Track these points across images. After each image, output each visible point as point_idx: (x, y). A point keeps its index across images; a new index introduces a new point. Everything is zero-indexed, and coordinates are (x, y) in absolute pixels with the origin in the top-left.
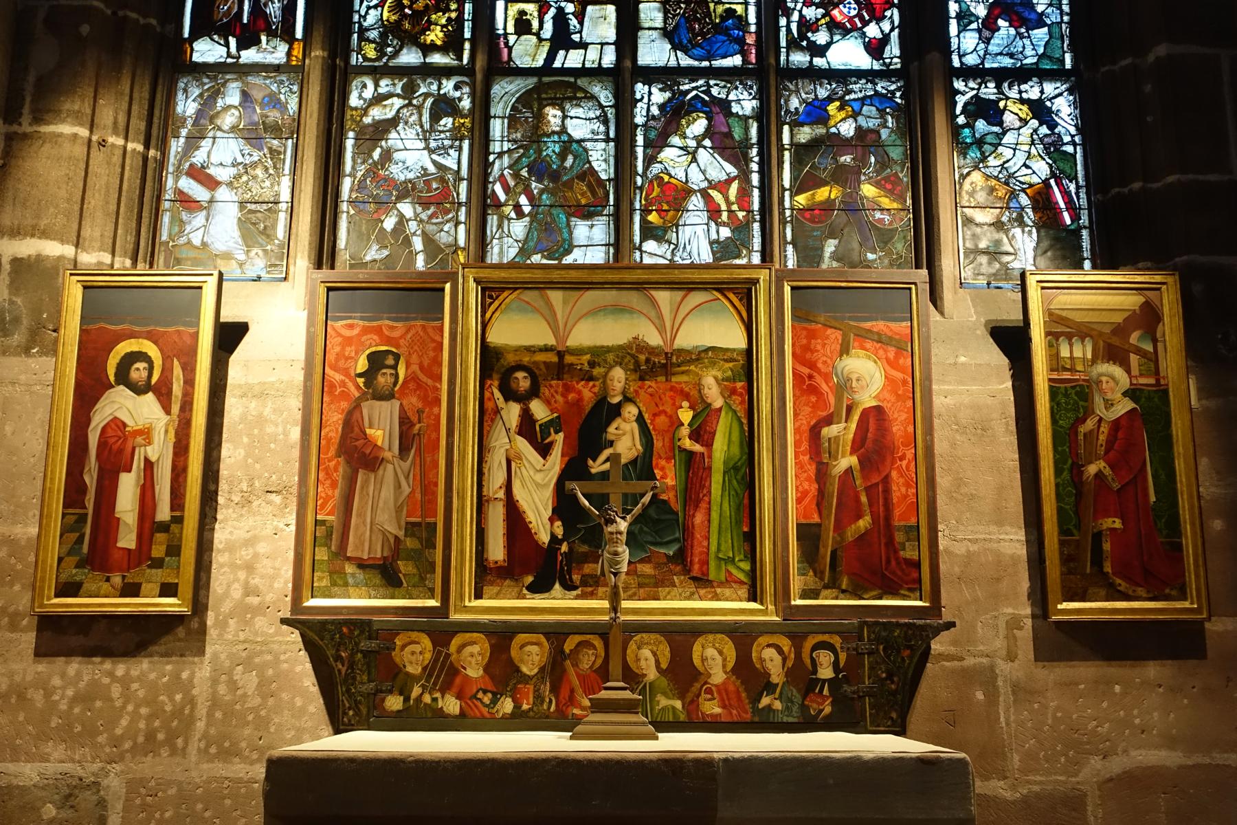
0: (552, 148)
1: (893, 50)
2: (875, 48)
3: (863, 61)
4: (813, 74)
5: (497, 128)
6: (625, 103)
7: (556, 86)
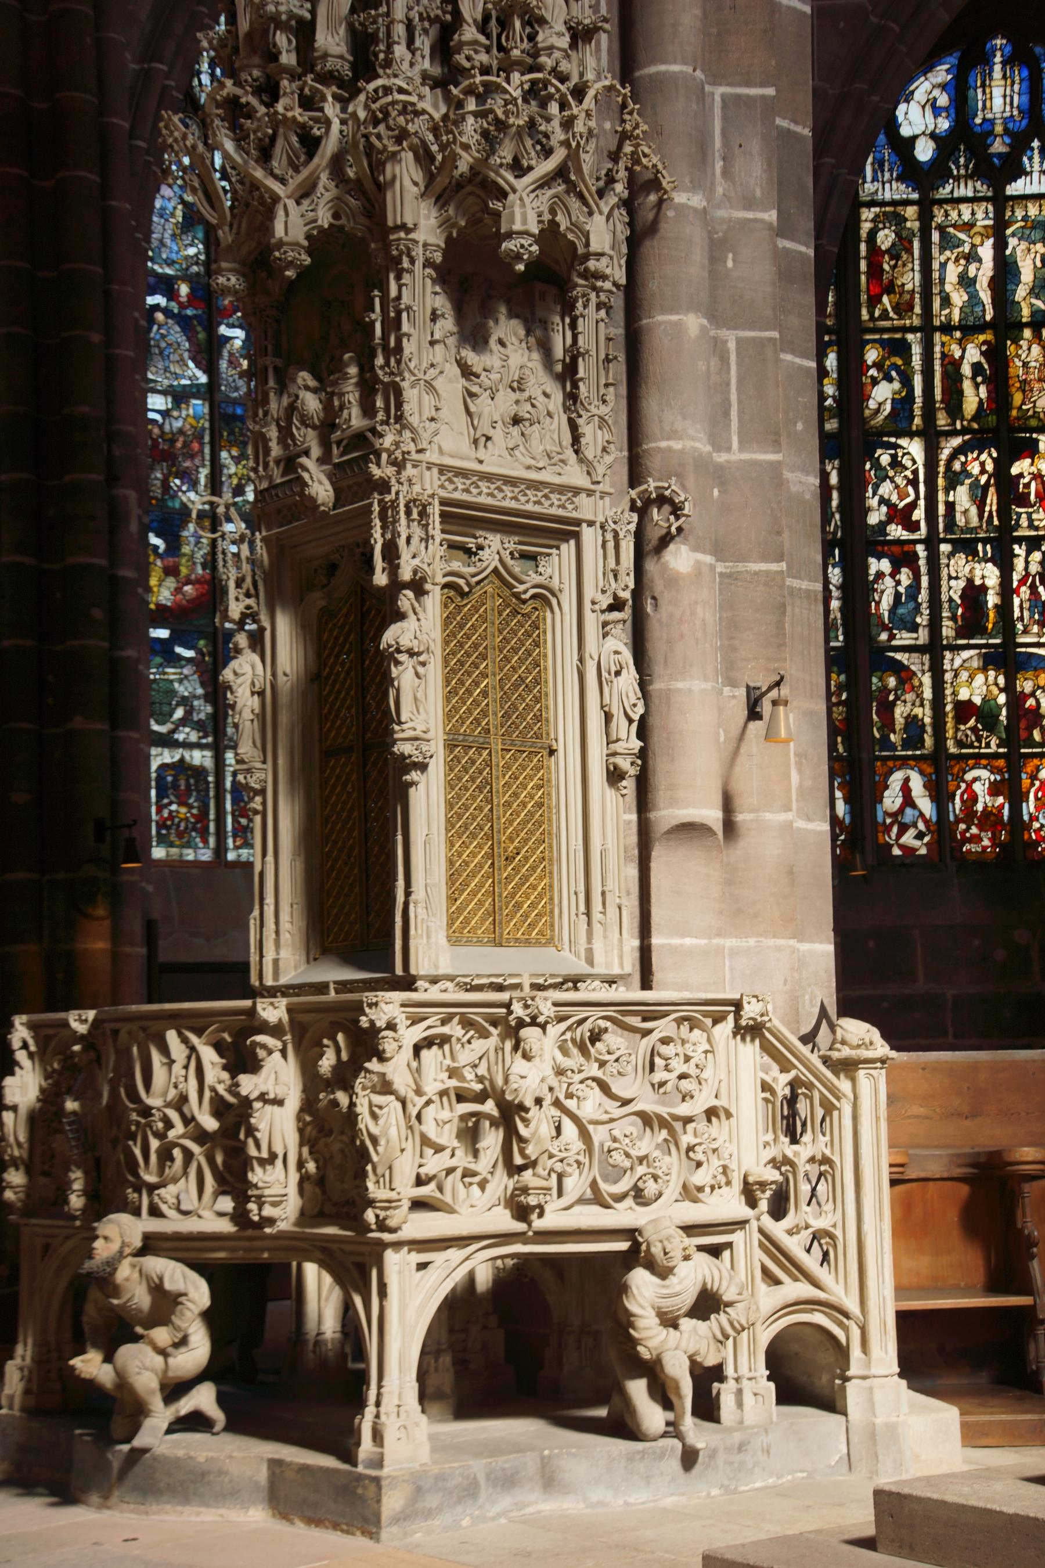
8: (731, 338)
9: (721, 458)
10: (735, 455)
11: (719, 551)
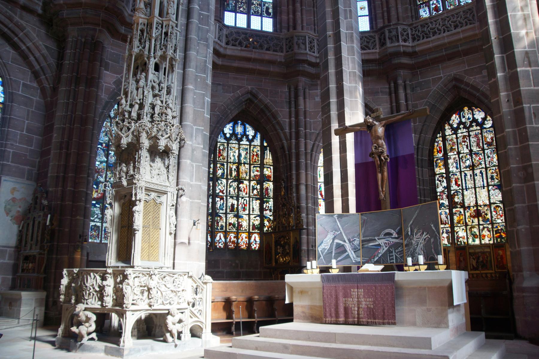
1: (504, 221)
2: (502, 220)
3: (501, 222)
5: (468, 231)
6: (479, 228)
7: (473, 227)
8: (194, 164)
9: (192, 183)
10: (194, 183)
11: (190, 198)
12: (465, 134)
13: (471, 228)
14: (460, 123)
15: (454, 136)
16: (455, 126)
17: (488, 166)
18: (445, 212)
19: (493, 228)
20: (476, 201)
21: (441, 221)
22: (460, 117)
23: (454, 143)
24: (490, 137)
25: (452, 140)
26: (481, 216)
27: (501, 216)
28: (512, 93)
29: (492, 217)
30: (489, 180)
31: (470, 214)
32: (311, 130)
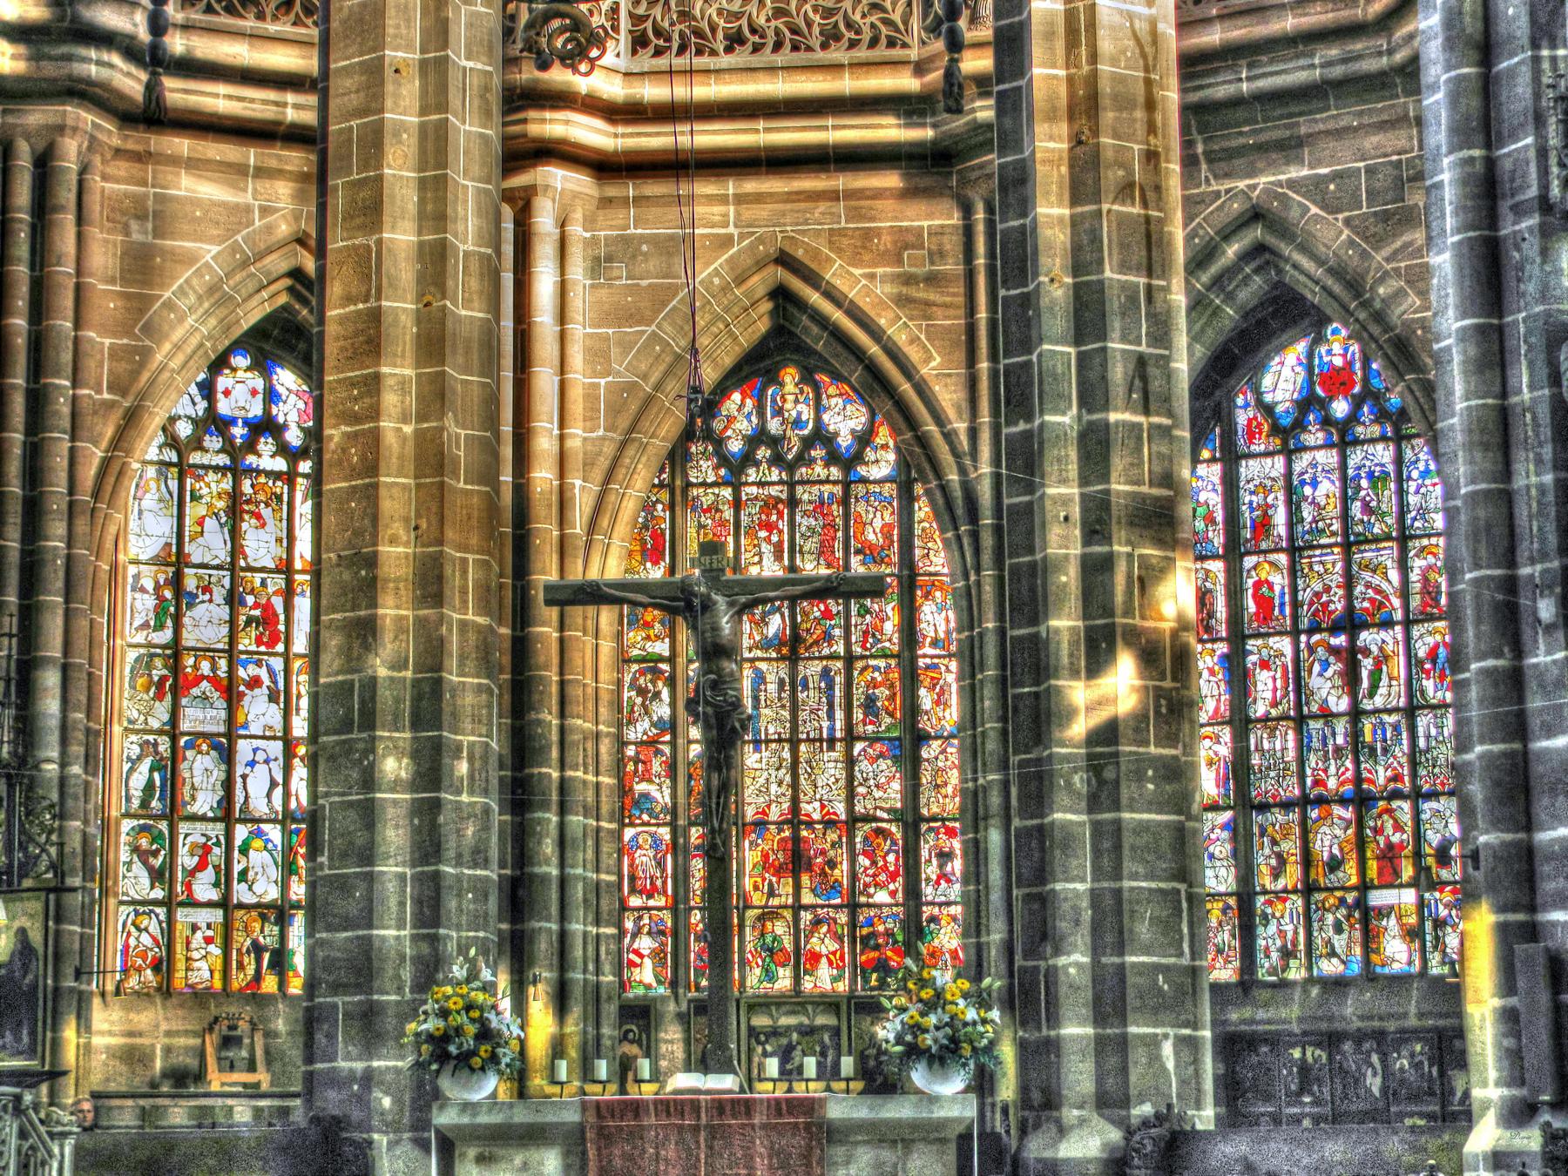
0: (769, 939)
1: (900, 895)
2: (893, 894)
3: (889, 900)
4: (869, 905)
6: (796, 919)
12: (774, 491)
13: (761, 918)
14: (760, 437)
15: (727, 493)
16: (735, 446)
17: (857, 650)
18: (652, 835)
19: (853, 924)
20: (795, 801)
21: (633, 878)
22: (760, 409)
23: (723, 523)
24: (878, 524)
25: (714, 508)
26: (810, 868)
27: (893, 877)
28: (1082, 495)
29: (854, 877)
30: (858, 715)
31: (765, 856)
32: (99, 392)
